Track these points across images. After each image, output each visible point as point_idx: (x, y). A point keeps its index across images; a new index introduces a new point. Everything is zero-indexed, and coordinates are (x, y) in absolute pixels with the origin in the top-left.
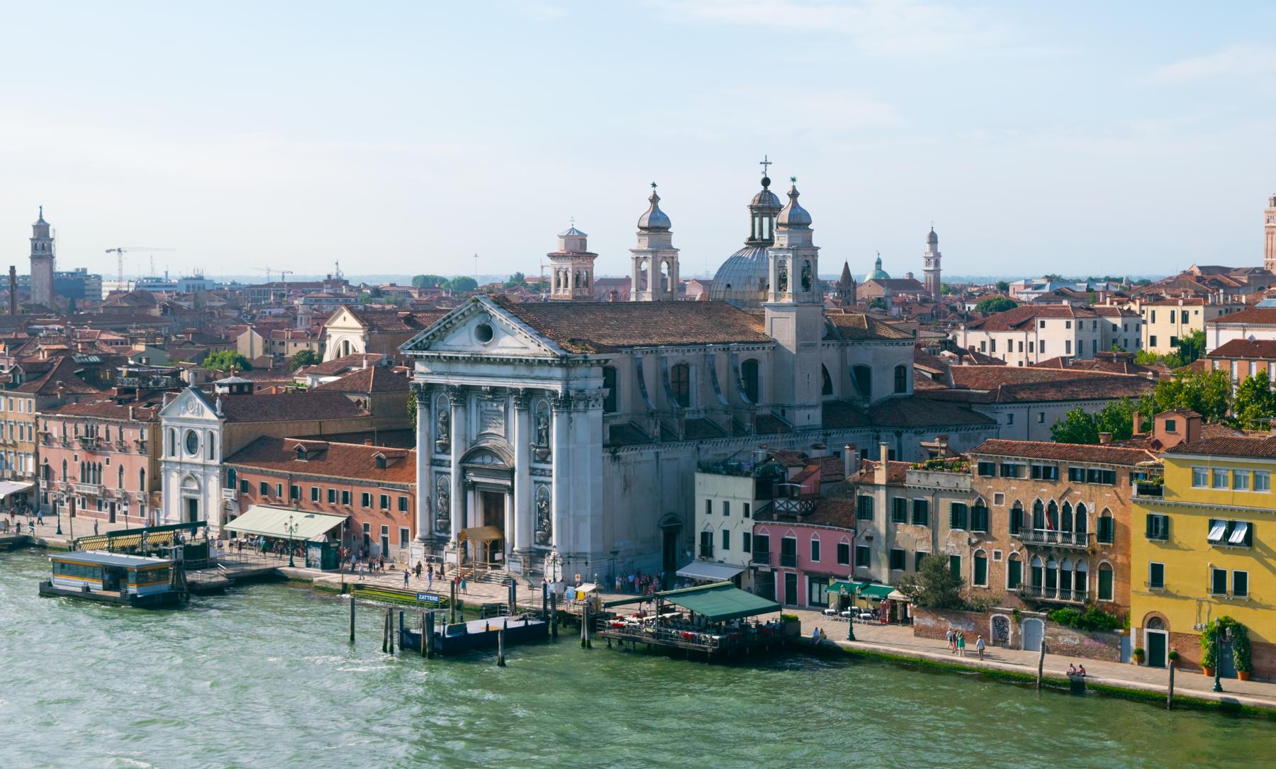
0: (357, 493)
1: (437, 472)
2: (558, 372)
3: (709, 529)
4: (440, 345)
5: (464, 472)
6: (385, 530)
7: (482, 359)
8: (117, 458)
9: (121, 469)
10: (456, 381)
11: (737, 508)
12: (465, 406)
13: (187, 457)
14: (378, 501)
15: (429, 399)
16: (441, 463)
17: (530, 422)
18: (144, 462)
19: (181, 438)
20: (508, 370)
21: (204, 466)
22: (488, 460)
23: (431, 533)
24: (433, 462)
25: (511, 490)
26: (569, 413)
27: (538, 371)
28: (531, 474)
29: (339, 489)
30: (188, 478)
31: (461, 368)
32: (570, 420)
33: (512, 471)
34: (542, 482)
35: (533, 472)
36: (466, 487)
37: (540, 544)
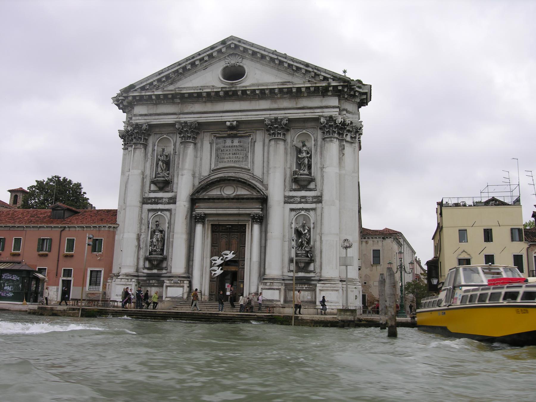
1: (149, 210)
2: (334, 101)
3: (464, 256)
6: (68, 273)
7: (235, 93)
11: (502, 235)
12: (195, 144)
15: (146, 140)
16: (157, 201)
17: (286, 153)
20: (264, 104)
22: (229, 192)
23: (137, 270)
24: (145, 201)
25: (262, 220)
26: (341, 140)
28: (285, 203)
31: (198, 107)
32: (342, 148)
33: (264, 201)
34: (302, 209)
35: (288, 200)
36: (194, 219)
37: (299, 269)
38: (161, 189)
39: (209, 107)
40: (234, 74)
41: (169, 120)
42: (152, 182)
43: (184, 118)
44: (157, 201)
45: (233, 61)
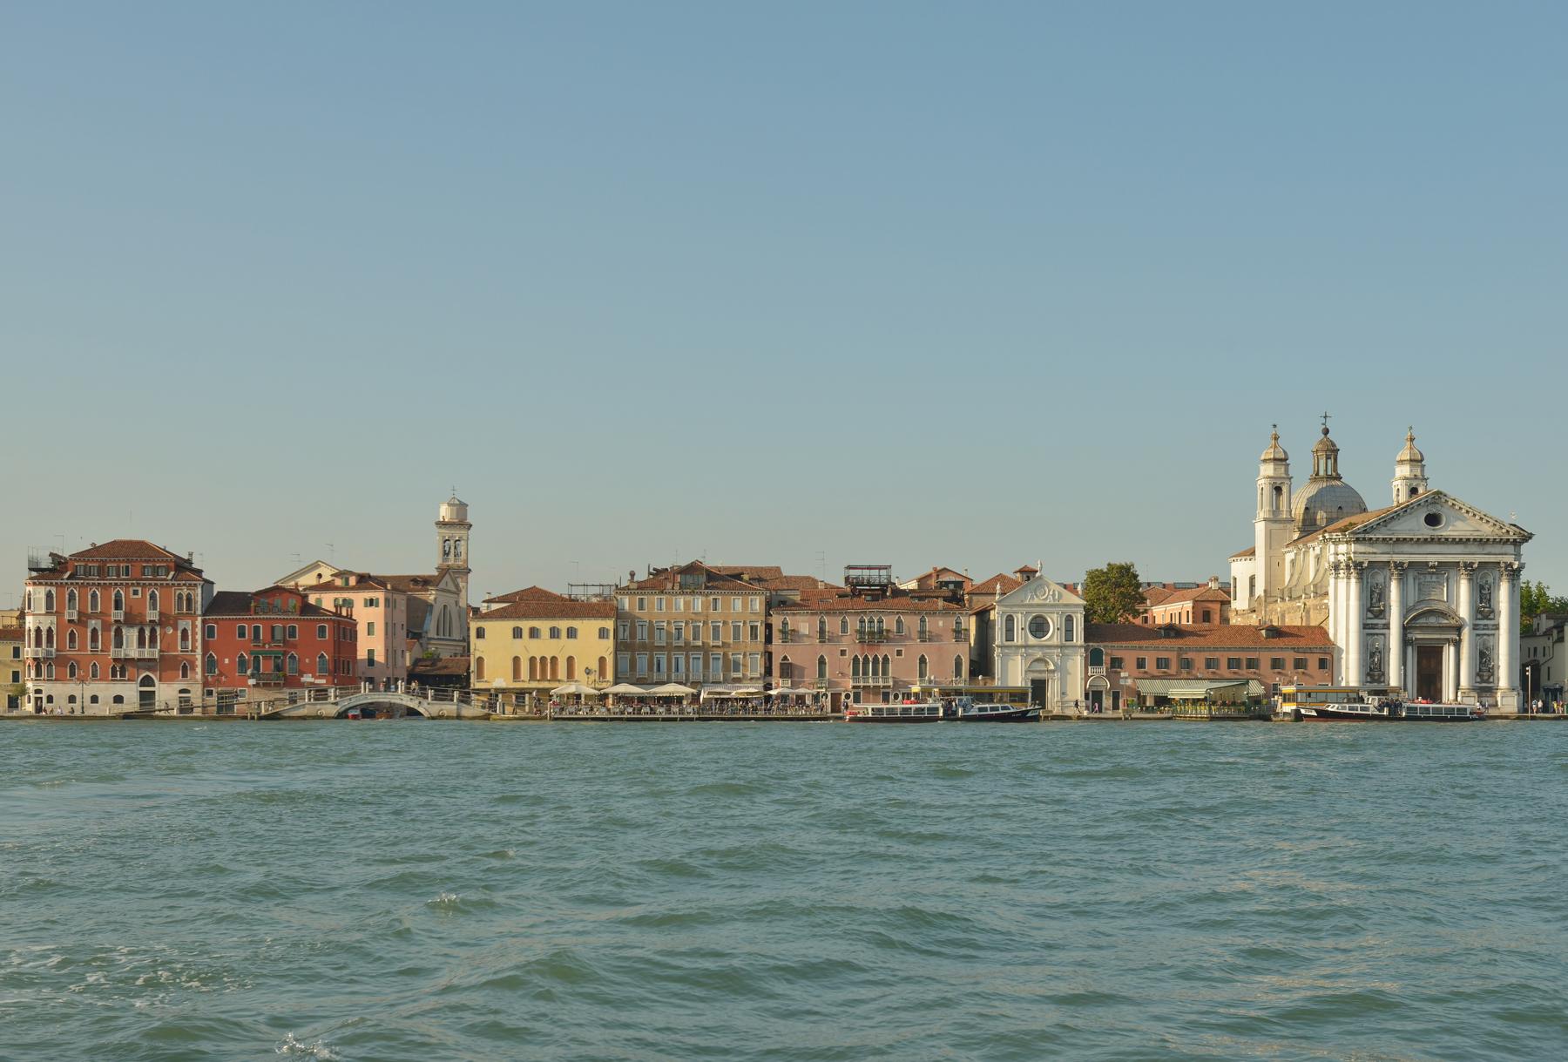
0: (1265, 659)
2: (1510, 549)
4: (1383, 529)
5: (1405, 629)
8: (916, 648)
9: (922, 660)
10: (1406, 559)
13: (1032, 640)
14: (1289, 665)
16: (1374, 626)
18: (964, 652)
19: (1020, 622)
20: (1459, 548)
21: (1061, 647)
22: (1432, 620)
24: (1365, 626)
25: (1457, 644)
27: (1489, 549)
29: (1244, 656)
30: (1038, 660)
31: (1406, 548)
33: (1459, 629)
35: (1475, 627)
36: (1405, 642)
37: (1483, 681)
38: (1376, 617)
39: (1415, 549)
40: (1433, 520)
41: (1385, 558)
42: (1369, 610)
43: (1398, 558)
44: (1374, 626)
45: (1433, 510)
